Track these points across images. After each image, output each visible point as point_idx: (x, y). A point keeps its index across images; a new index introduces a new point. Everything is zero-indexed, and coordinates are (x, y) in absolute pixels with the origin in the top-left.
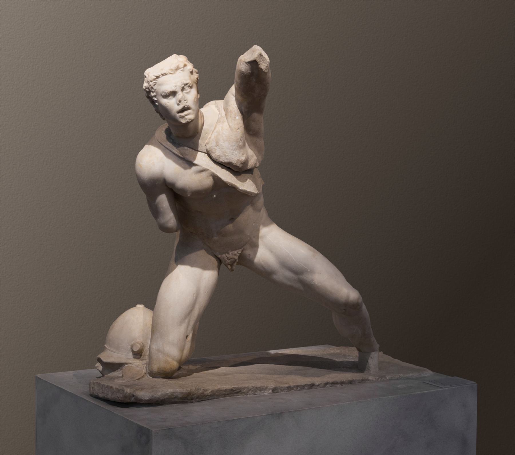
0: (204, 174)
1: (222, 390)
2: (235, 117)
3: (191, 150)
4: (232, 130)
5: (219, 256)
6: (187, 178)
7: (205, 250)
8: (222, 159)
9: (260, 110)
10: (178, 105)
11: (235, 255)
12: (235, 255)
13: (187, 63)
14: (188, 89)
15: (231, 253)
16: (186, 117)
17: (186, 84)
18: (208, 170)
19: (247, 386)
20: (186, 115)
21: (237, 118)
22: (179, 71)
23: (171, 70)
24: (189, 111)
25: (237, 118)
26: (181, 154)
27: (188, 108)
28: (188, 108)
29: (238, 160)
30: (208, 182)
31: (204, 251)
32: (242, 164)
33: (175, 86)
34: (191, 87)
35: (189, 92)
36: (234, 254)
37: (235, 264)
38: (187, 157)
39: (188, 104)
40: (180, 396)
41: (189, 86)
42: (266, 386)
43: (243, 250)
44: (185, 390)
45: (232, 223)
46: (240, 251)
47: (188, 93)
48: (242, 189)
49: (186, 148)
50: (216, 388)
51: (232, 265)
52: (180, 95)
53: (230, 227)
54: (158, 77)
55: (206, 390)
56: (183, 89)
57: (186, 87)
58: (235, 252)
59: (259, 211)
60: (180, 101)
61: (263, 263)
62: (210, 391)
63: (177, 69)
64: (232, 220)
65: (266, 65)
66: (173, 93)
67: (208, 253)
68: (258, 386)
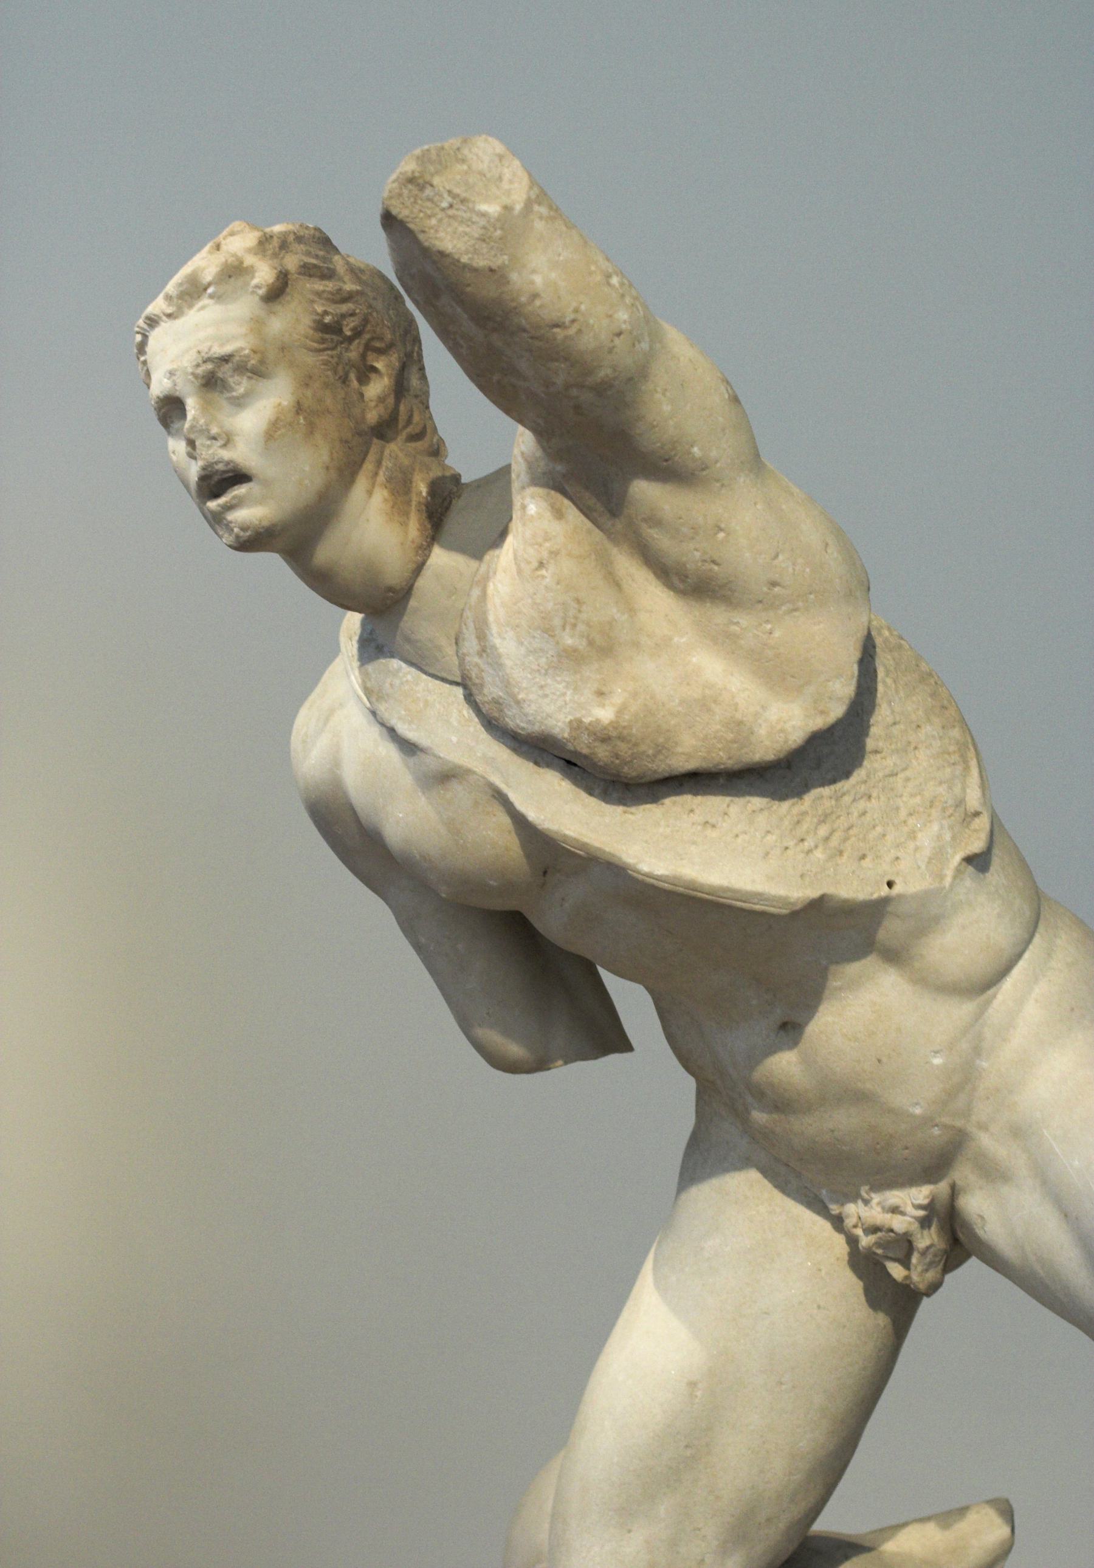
0: (457, 790)
2: (524, 507)
4: (520, 571)
5: (835, 1209)
6: (407, 817)
7: (765, 1172)
8: (514, 720)
10: (192, 456)
11: (895, 1210)
12: (895, 1210)
13: (250, 260)
14: (241, 385)
15: (876, 1198)
17: (225, 359)
18: (469, 771)
20: (229, 507)
22: (205, 301)
24: (241, 490)
26: (368, 692)
28: (238, 477)
29: (577, 725)
30: (495, 838)
31: (754, 1175)
32: (605, 739)
33: (172, 373)
35: (247, 395)
36: (901, 1208)
37: (914, 1260)
38: (382, 708)
39: (226, 454)
41: (242, 368)
45: (794, 1043)
46: (921, 1194)
47: (239, 403)
49: (395, 663)
53: (785, 1065)
57: (225, 371)
58: (895, 1197)
60: (191, 443)
61: (1037, 1267)
64: (790, 1030)
65: (476, 232)
66: (171, 409)
67: (783, 1187)
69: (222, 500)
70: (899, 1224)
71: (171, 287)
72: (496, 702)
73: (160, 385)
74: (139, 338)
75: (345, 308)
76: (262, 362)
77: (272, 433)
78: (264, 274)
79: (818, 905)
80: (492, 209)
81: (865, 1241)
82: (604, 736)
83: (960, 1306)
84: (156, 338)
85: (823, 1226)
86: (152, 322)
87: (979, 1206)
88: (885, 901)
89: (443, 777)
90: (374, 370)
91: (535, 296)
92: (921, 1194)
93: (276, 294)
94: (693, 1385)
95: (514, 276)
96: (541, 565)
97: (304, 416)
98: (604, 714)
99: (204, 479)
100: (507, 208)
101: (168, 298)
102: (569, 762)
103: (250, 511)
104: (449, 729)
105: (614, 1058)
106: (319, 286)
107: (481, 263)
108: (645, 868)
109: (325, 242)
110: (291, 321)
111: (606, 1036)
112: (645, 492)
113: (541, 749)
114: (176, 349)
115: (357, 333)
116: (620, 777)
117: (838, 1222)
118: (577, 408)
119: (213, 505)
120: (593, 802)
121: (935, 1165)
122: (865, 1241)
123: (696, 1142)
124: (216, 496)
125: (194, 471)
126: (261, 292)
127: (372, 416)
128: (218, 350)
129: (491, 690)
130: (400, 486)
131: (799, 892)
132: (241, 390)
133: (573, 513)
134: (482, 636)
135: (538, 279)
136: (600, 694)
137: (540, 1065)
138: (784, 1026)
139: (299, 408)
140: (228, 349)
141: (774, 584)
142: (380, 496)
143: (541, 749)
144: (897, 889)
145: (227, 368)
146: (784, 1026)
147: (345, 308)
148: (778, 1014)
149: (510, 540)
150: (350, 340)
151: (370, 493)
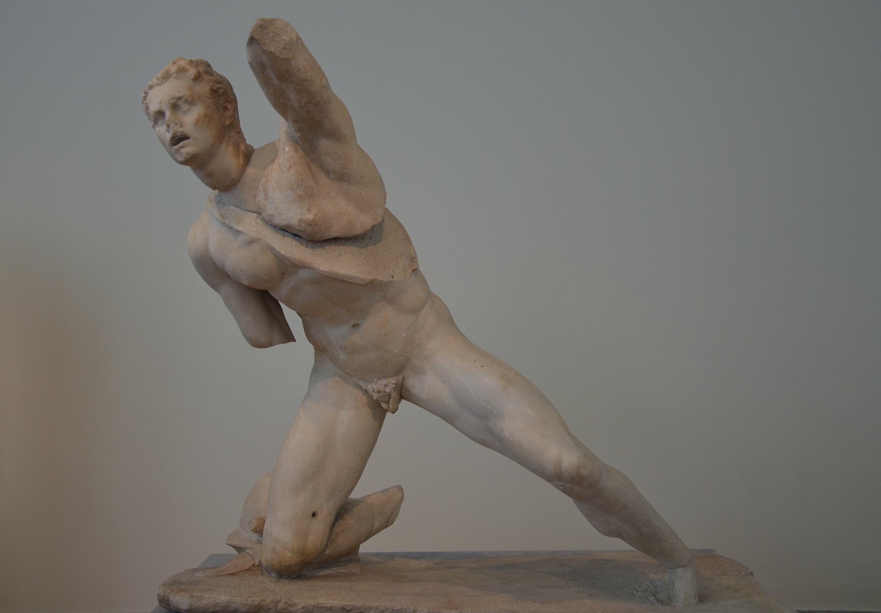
1: (323, 608)
2: (284, 149)
3: (238, 210)
6: (236, 258)
8: (278, 220)
9: (335, 135)
10: (168, 131)
13: (187, 67)
14: (185, 107)
16: (182, 150)
17: (180, 98)
19: (374, 604)
20: (182, 147)
21: (287, 149)
22: (172, 79)
23: (158, 79)
24: (187, 141)
25: (287, 149)
26: (222, 216)
27: (185, 137)
28: (185, 137)
29: (301, 220)
30: (266, 262)
32: (310, 225)
34: (192, 103)
35: (188, 110)
36: (387, 384)
38: (226, 221)
39: (181, 130)
40: (243, 609)
41: (186, 101)
42: (412, 609)
43: (404, 378)
44: (250, 600)
46: (393, 380)
48: (325, 270)
50: (312, 602)
51: (387, 403)
52: (168, 114)
54: (146, 93)
55: (295, 605)
56: (175, 107)
57: (180, 103)
58: (384, 382)
59: (416, 311)
60: (168, 126)
62: (300, 606)
63: (167, 76)
66: (160, 114)
68: (397, 608)
69: (179, 145)
70: (388, 390)
71: (159, 75)
72: (271, 216)
73: (154, 107)
74: (144, 95)
75: (219, 86)
76: (193, 99)
77: (197, 123)
78: (192, 72)
79: (372, 282)
80: (287, 38)
81: (375, 396)
82: (310, 224)
83: (404, 418)
84: (151, 93)
85: (359, 394)
86: (151, 87)
87: (414, 384)
88: (391, 282)
89: (251, 242)
90: (227, 108)
91: (299, 70)
92: (393, 380)
93: (197, 78)
94: (319, 447)
95: (293, 62)
96: (290, 167)
97: (205, 120)
98: (310, 216)
99: (173, 138)
100: (292, 39)
101: (158, 79)
102: (295, 235)
103: (188, 149)
104: (250, 225)
105: (291, 343)
106: (211, 77)
107: (282, 56)
108: (321, 269)
109: (210, 66)
110: (203, 88)
111: (288, 337)
112: (324, 144)
113: (285, 230)
114: (159, 98)
115: (223, 94)
116: (314, 238)
117: (365, 392)
118: (308, 112)
119: (176, 147)
120: (303, 247)
121: (400, 370)
122: (375, 396)
123: (315, 371)
124: (175, 145)
125: (168, 136)
126: (192, 77)
127: (228, 122)
128: (178, 95)
129: (270, 210)
130: (237, 147)
131: (368, 277)
132: (186, 108)
133: (300, 151)
134: (266, 194)
135: (300, 64)
136: (309, 210)
137: (270, 345)
138: (354, 326)
139: (206, 116)
140: (181, 95)
141: (362, 177)
142: (231, 148)
143: (285, 230)
144: (395, 278)
145: (181, 101)
146: (354, 326)
147: (219, 86)
148: (353, 322)
149: (277, 161)
150: (221, 96)
151: (227, 147)
